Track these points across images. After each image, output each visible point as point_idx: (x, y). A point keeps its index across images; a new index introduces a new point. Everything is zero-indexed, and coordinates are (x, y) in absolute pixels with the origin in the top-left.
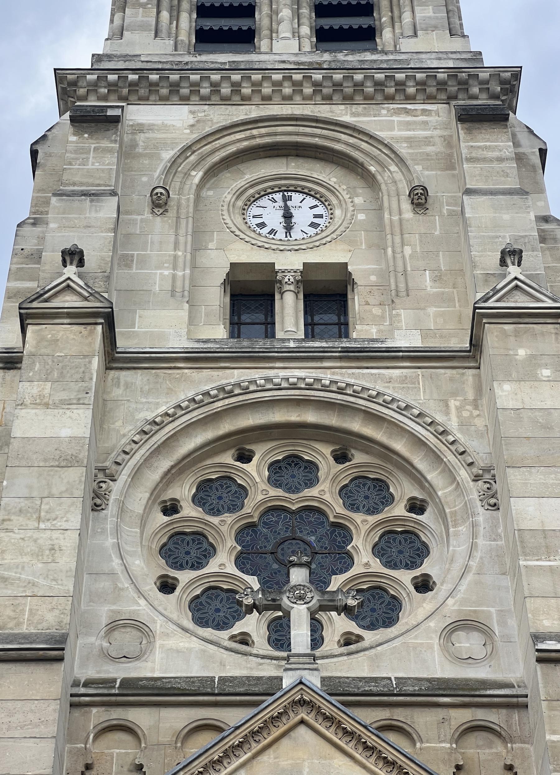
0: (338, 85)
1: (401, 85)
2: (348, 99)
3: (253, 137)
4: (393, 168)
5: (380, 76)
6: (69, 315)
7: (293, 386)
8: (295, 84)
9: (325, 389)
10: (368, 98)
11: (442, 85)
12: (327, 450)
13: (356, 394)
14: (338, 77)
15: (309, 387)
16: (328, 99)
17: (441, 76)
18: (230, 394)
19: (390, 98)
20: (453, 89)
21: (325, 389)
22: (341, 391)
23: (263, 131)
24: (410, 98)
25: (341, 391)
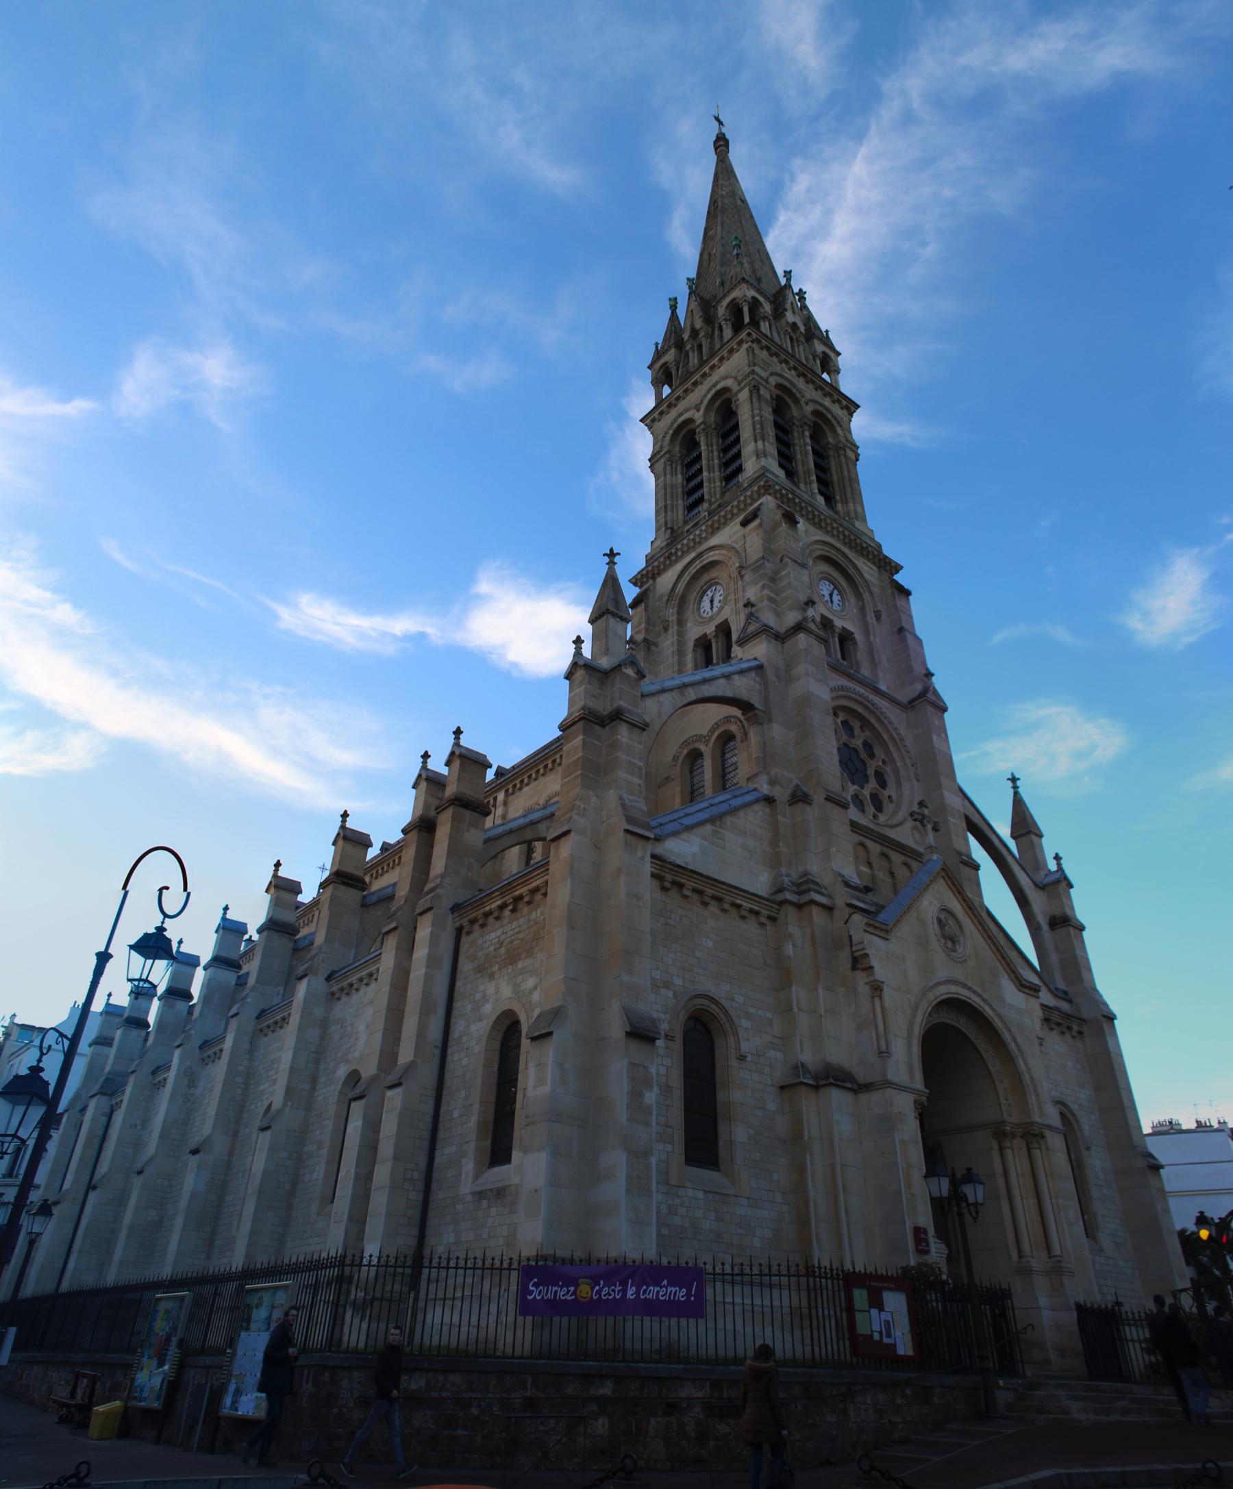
0: (850, 540)
1: (868, 552)
2: (851, 548)
3: (830, 552)
4: (867, 594)
5: (865, 545)
6: (816, 636)
7: (860, 696)
8: (833, 528)
9: (868, 701)
10: (857, 551)
11: (880, 560)
12: (859, 724)
13: (877, 708)
14: (852, 537)
15: (864, 698)
16: (845, 544)
17: (882, 557)
18: (843, 690)
19: (862, 555)
20: (882, 564)
21: (868, 701)
22: (873, 705)
23: (827, 549)
24: (868, 559)
25: (873, 705)
